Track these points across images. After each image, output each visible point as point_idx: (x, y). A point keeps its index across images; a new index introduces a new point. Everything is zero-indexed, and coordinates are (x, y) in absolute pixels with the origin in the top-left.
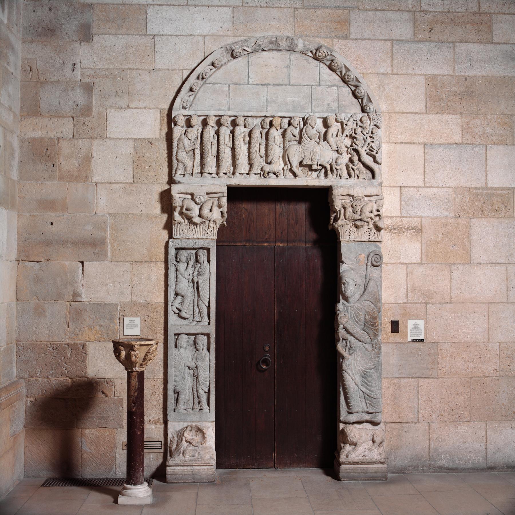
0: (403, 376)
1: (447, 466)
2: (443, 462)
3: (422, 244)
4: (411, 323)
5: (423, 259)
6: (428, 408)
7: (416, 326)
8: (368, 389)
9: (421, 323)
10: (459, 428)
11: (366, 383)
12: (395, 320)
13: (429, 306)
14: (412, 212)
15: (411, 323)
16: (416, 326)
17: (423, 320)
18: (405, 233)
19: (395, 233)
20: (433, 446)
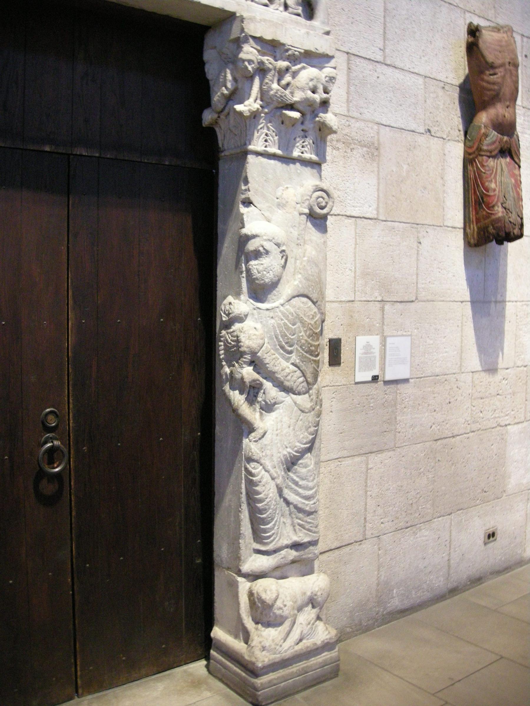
0: (345, 453)
1: (401, 607)
2: (396, 603)
3: (379, 179)
4: (361, 341)
5: (381, 211)
6: (379, 508)
7: (368, 347)
8: (298, 494)
9: (375, 340)
10: (418, 535)
11: (296, 483)
12: (335, 337)
13: (387, 307)
14: (366, 111)
15: (361, 341)
16: (368, 347)
17: (378, 337)
18: (355, 152)
19: (338, 149)
20: (383, 577)
